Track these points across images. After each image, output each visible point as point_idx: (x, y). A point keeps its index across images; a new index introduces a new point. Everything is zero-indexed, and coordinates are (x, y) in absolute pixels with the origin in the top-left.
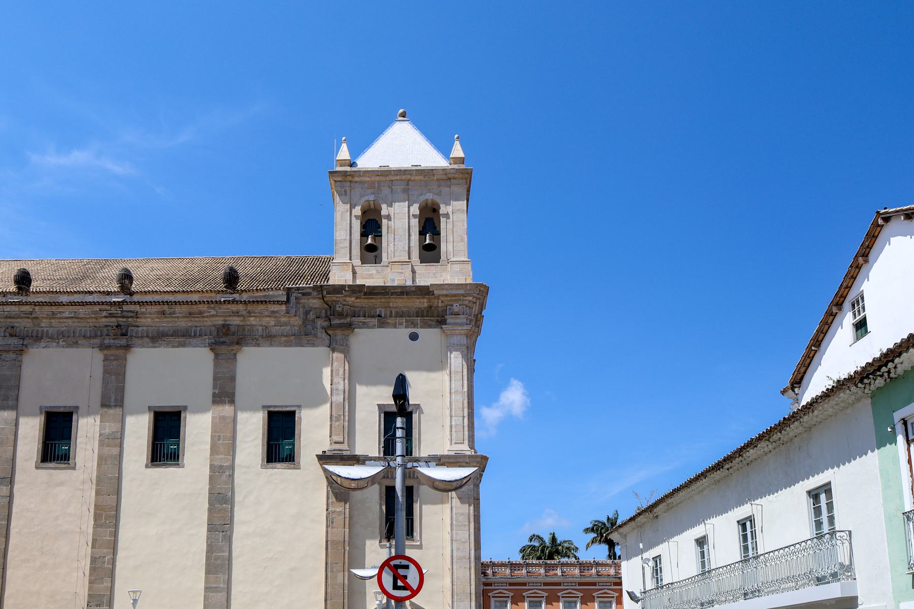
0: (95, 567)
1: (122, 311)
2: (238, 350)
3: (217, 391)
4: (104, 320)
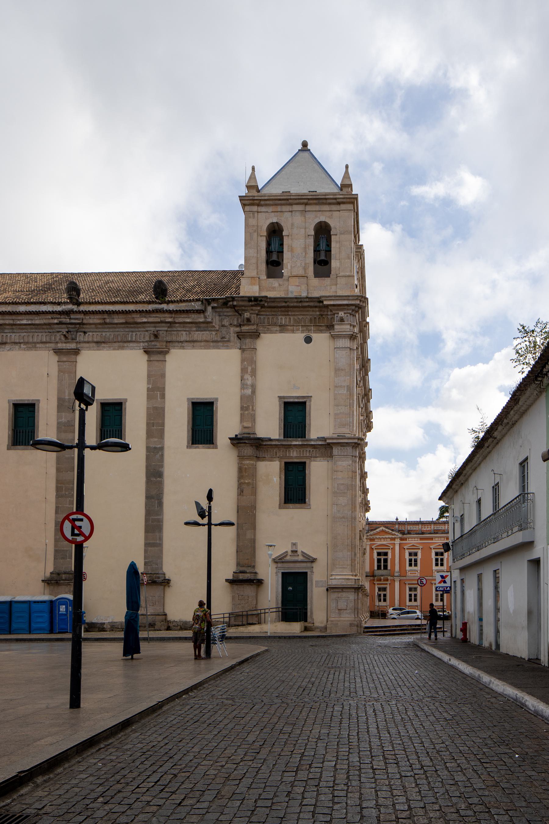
3: (150, 386)
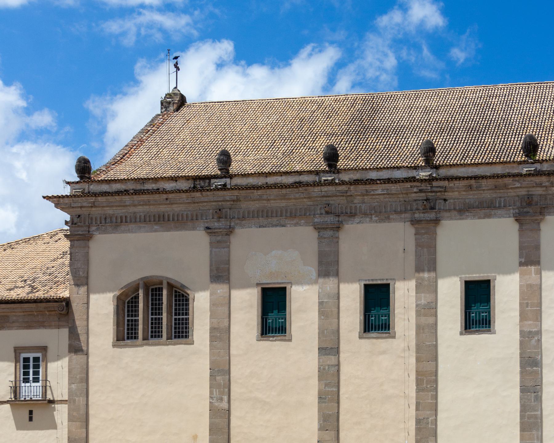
0: (419, 427)
1: (432, 187)
2: (542, 220)
3: (523, 260)
4: (414, 195)
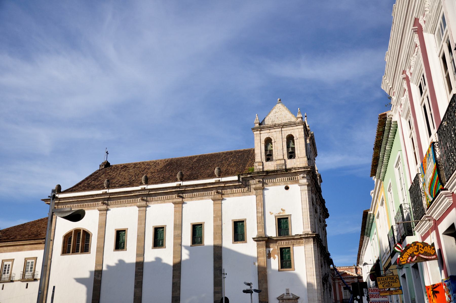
3: (215, 216)
